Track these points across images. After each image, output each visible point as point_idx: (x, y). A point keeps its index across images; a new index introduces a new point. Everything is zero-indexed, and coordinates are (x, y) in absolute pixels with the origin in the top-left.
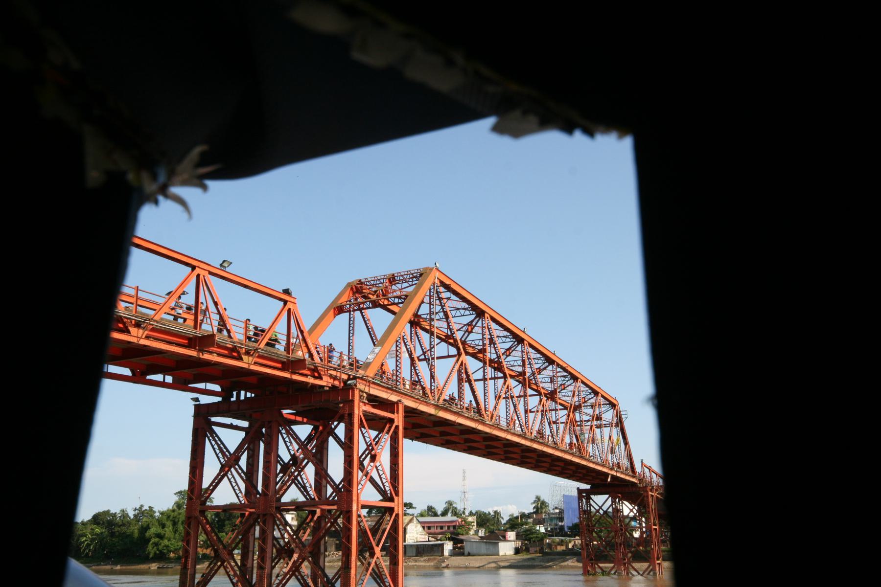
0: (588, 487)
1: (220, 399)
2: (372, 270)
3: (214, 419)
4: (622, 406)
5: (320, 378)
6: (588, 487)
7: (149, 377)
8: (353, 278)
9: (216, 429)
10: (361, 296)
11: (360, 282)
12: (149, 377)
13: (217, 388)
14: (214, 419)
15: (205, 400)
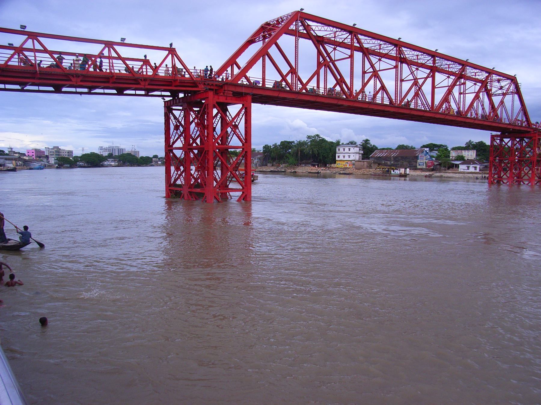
0: (499, 133)
1: (171, 98)
2: (271, 16)
3: (174, 108)
4: (519, 81)
5: (196, 86)
6: (499, 133)
7: (125, 92)
8: (263, 22)
9: (174, 111)
10: (268, 32)
11: (268, 24)
12: (125, 92)
13: (168, 94)
14: (174, 108)
15: (167, 99)
